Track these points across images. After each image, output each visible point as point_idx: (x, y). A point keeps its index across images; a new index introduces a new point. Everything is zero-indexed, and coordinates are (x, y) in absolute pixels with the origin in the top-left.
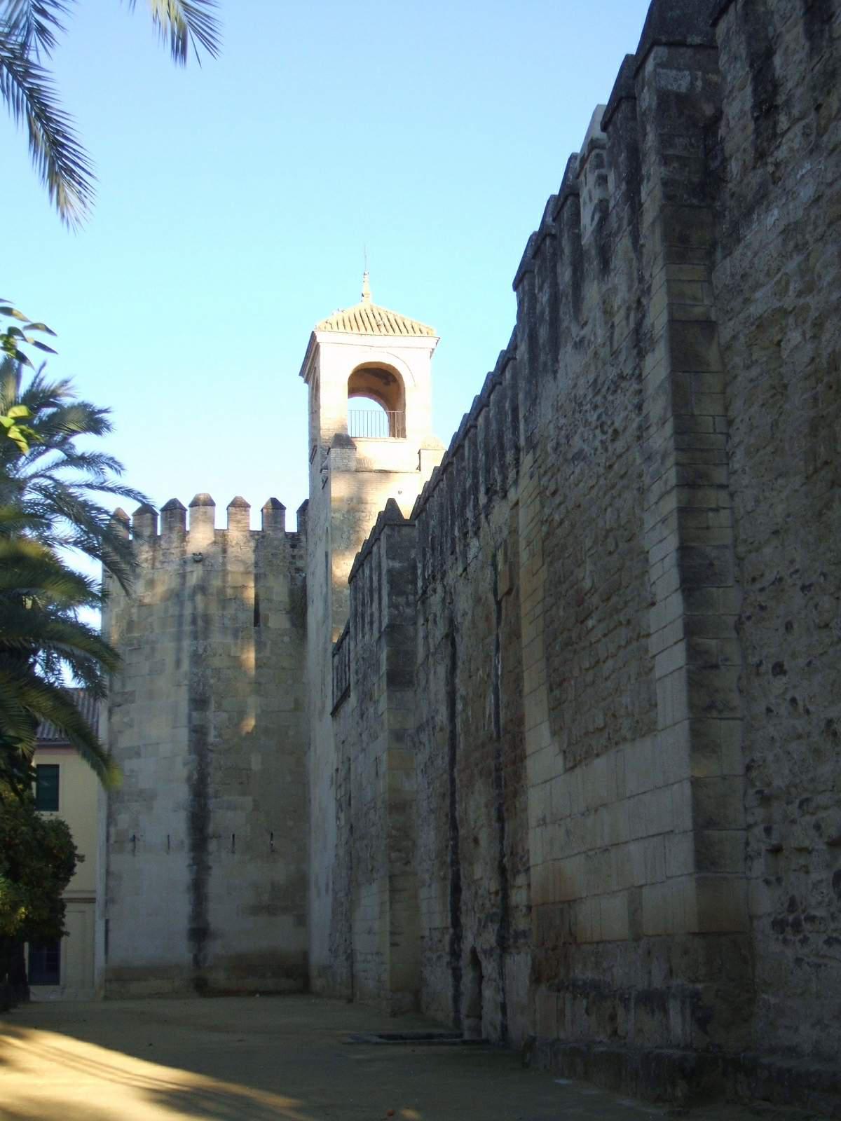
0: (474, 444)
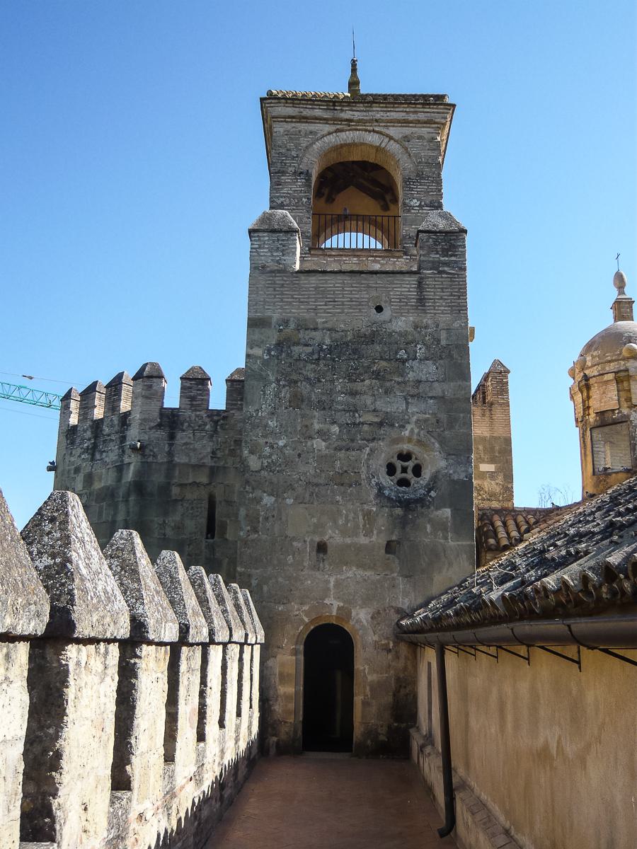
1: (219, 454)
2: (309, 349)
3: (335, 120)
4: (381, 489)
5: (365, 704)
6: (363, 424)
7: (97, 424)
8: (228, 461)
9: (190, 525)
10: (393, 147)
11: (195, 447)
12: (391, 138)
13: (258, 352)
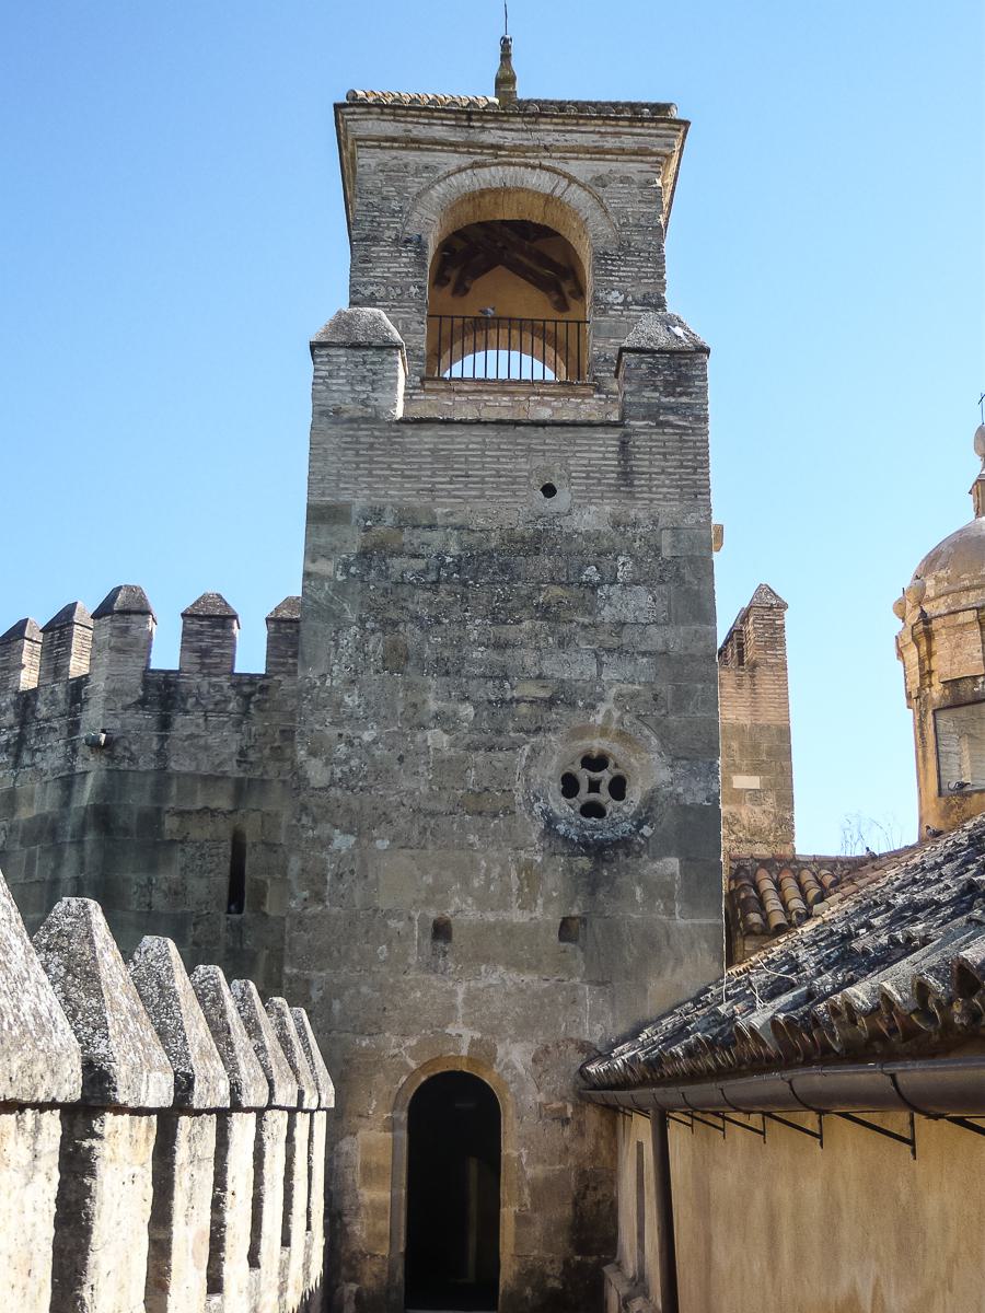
1: (253, 756)
2: (420, 564)
3: (471, 146)
4: (551, 821)
5: (522, 1220)
6: (518, 701)
8: (269, 768)
9: (198, 887)
10: (576, 196)
11: (208, 743)
12: (572, 180)
13: (325, 567)
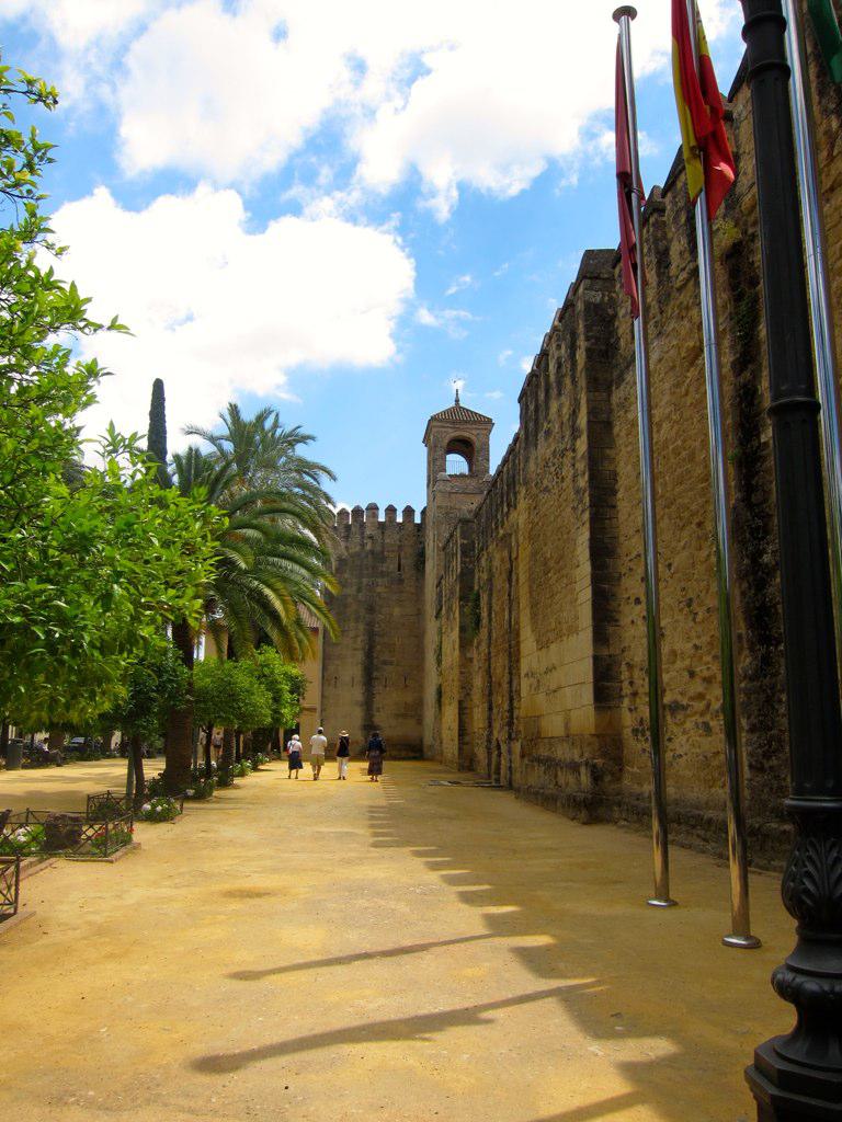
0: (502, 480)
7: (348, 527)
9: (391, 566)
10: (473, 438)
